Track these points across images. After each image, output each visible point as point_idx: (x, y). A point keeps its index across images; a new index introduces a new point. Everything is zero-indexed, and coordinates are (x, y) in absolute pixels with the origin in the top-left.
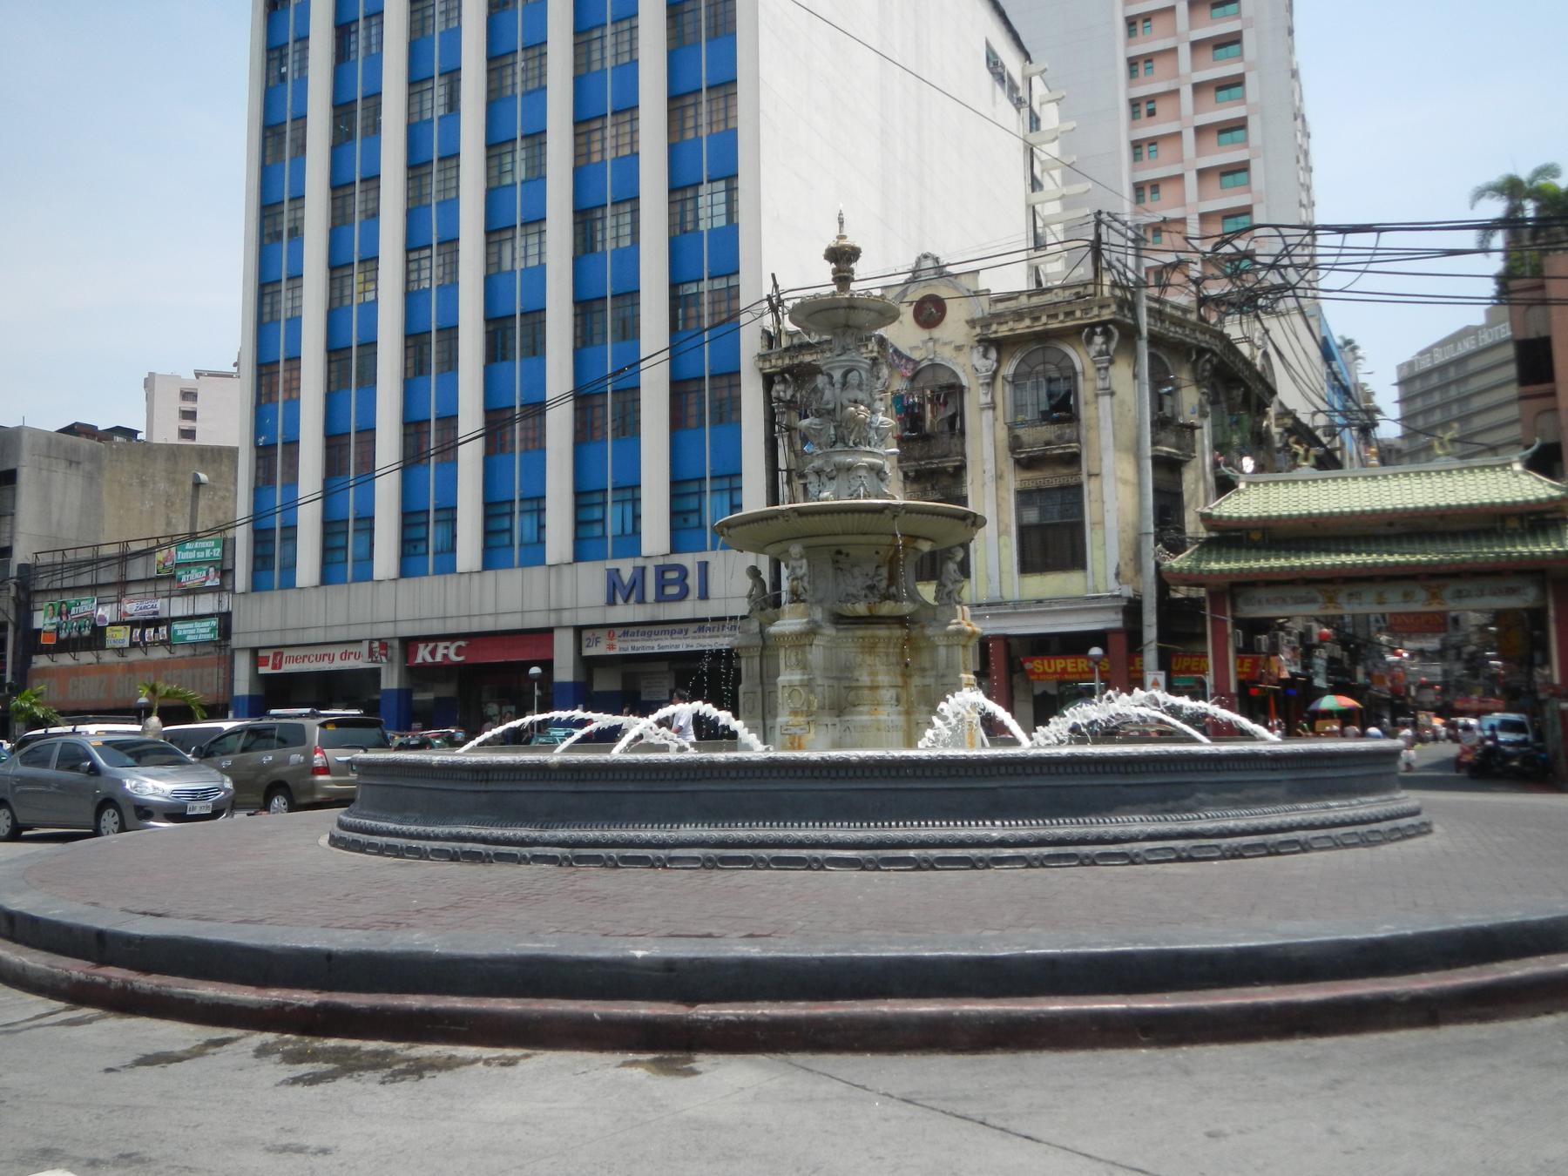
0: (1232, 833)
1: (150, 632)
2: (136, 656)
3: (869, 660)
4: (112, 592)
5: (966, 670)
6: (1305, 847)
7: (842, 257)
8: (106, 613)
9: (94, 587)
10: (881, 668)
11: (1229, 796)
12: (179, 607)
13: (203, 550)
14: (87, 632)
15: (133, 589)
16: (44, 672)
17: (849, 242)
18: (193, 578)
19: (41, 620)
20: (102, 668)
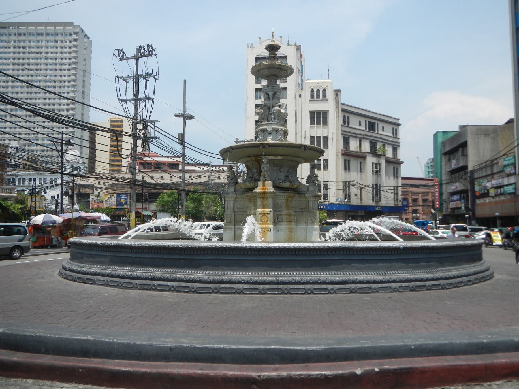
0: (79, 272)
1: (499, 190)
2: (497, 199)
3: (250, 205)
4: (490, 177)
5: (264, 207)
6: (93, 282)
7: (273, 48)
8: (489, 185)
9: (486, 176)
10: (253, 207)
11: (91, 259)
12: (506, 181)
13: (509, 160)
14: (486, 191)
15: (496, 176)
16: (478, 204)
17: (277, 42)
18: (508, 170)
19: (477, 188)
20: (490, 203)
